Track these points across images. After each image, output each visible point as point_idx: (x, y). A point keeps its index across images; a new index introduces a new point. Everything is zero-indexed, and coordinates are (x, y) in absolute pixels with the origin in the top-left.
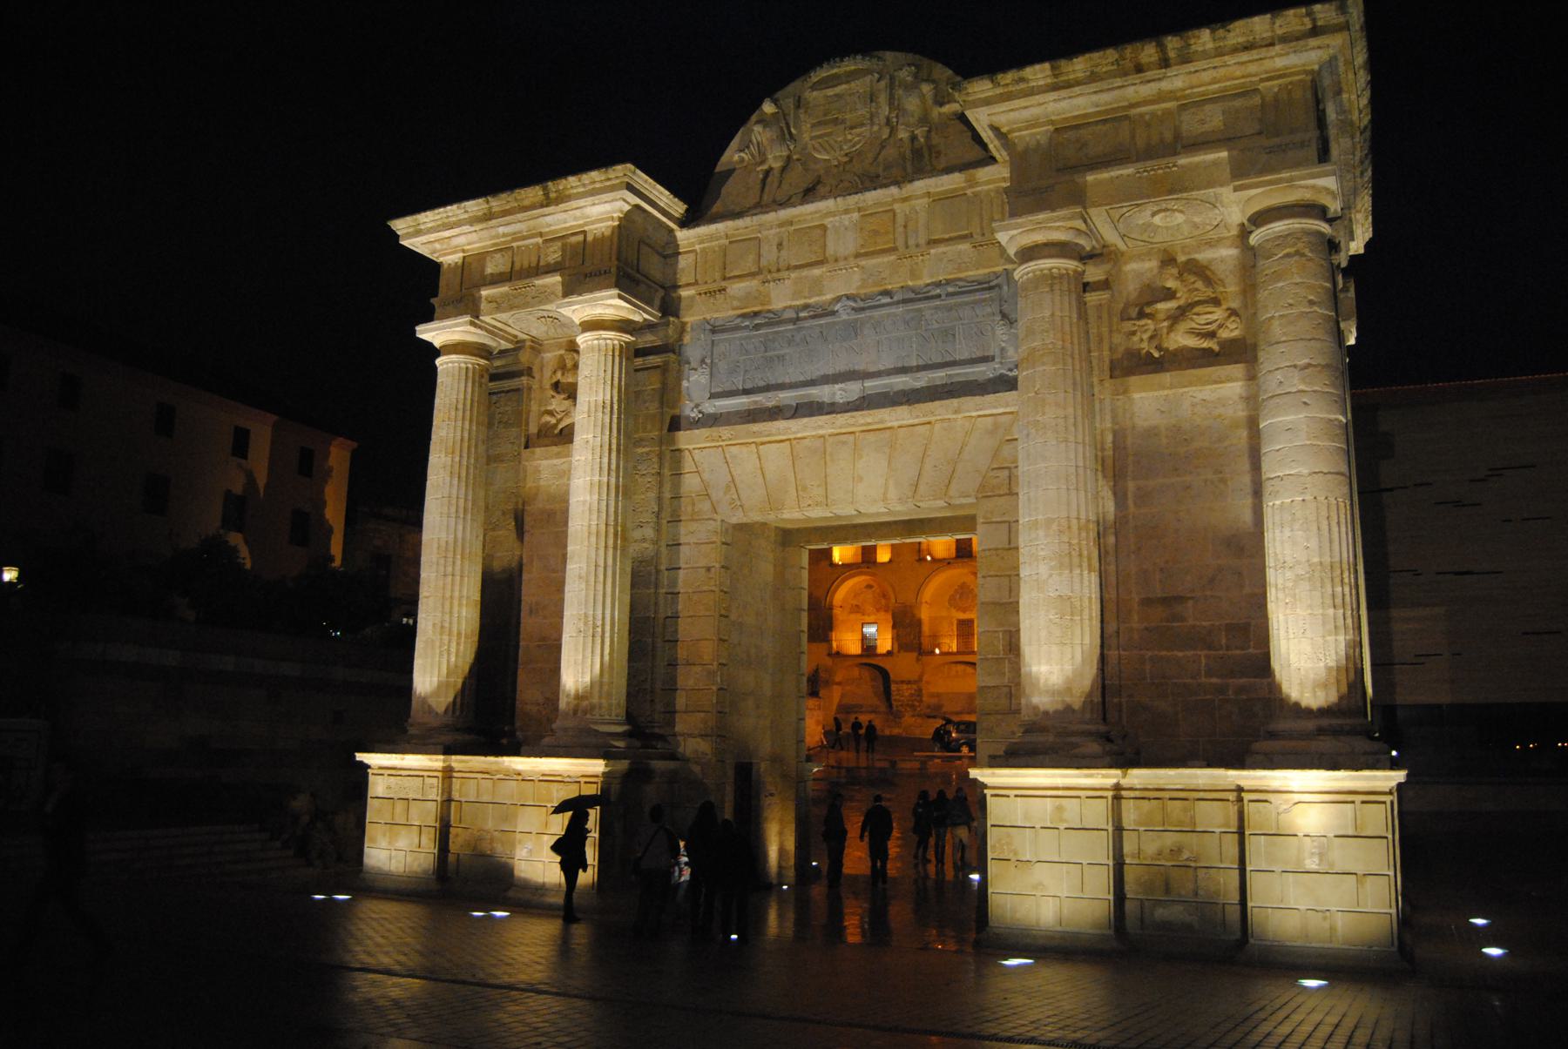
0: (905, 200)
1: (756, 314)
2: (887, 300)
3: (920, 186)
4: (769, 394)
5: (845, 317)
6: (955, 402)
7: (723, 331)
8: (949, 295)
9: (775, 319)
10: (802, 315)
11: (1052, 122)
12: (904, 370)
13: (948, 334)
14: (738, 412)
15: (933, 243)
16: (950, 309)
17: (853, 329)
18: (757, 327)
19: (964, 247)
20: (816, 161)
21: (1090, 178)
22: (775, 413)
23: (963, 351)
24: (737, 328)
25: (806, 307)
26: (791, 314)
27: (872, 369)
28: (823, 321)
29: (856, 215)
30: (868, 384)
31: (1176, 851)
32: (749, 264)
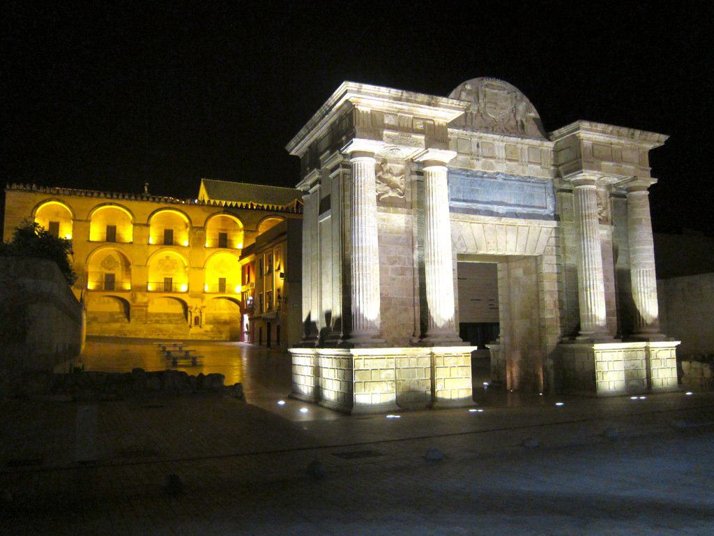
0: (522, 144)
1: (467, 171)
2: (513, 178)
3: (527, 141)
4: (475, 204)
5: (500, 181)
6: (538, 221)
7: (455, 174)
8: (533, 182)
9: (474, 175)
10: (485, 175)
11: (592, 141)
12: (519, 206)
13: (531, 196)
14: (461, 208)
15: (530, 162)
16: (533, 187)
17: (501, 186)
18: (468, 176)
19: (539, 167)
20: (488, 116)
21: (603, 163)
22: (476, 212)
23: (537, 203)
24: (459, 174)
25: (485, 173)
26: (479, 174)
27: (509, 202)
28: (492, 180)
29: (505, 143)
30: (509, 208)
31: (633, 366)
32: (466, 150)
